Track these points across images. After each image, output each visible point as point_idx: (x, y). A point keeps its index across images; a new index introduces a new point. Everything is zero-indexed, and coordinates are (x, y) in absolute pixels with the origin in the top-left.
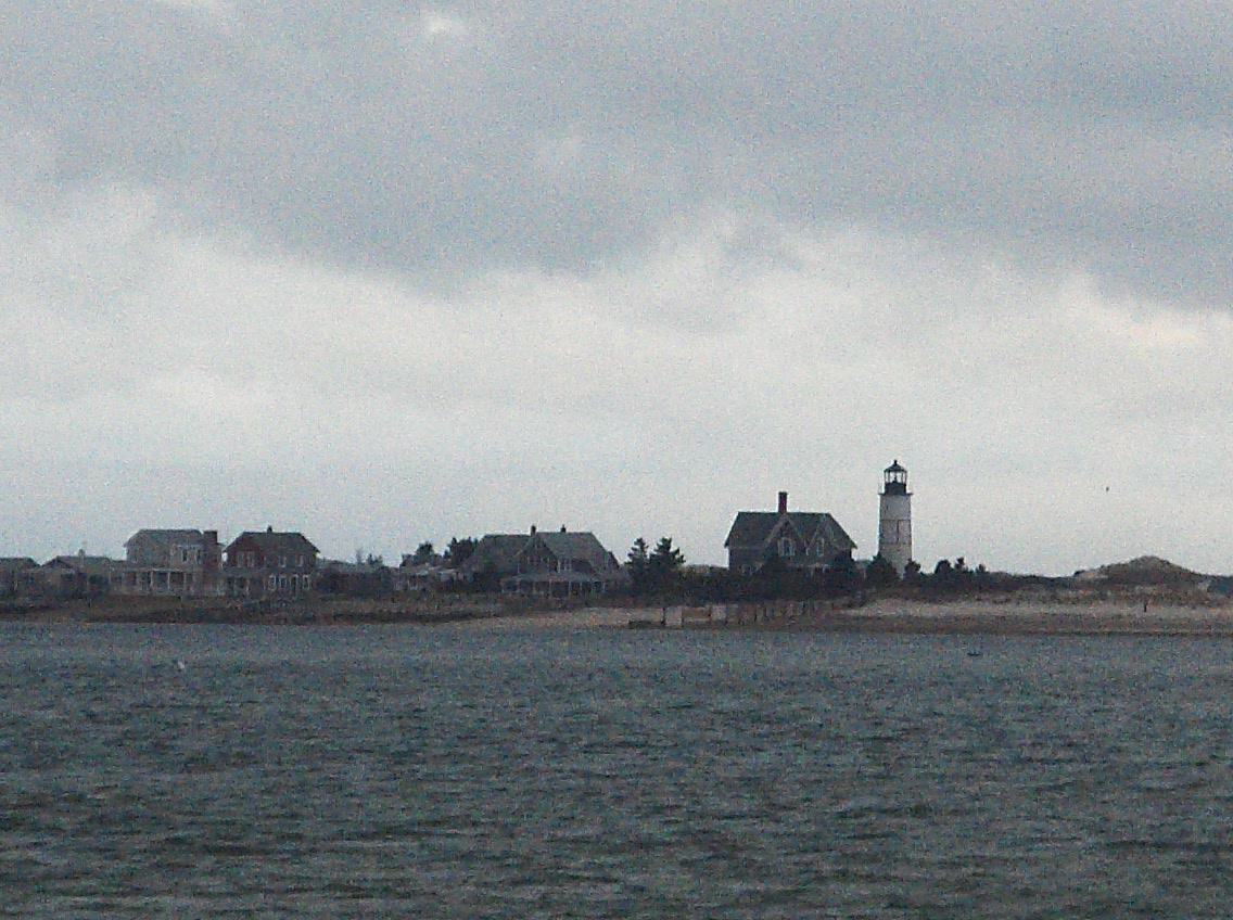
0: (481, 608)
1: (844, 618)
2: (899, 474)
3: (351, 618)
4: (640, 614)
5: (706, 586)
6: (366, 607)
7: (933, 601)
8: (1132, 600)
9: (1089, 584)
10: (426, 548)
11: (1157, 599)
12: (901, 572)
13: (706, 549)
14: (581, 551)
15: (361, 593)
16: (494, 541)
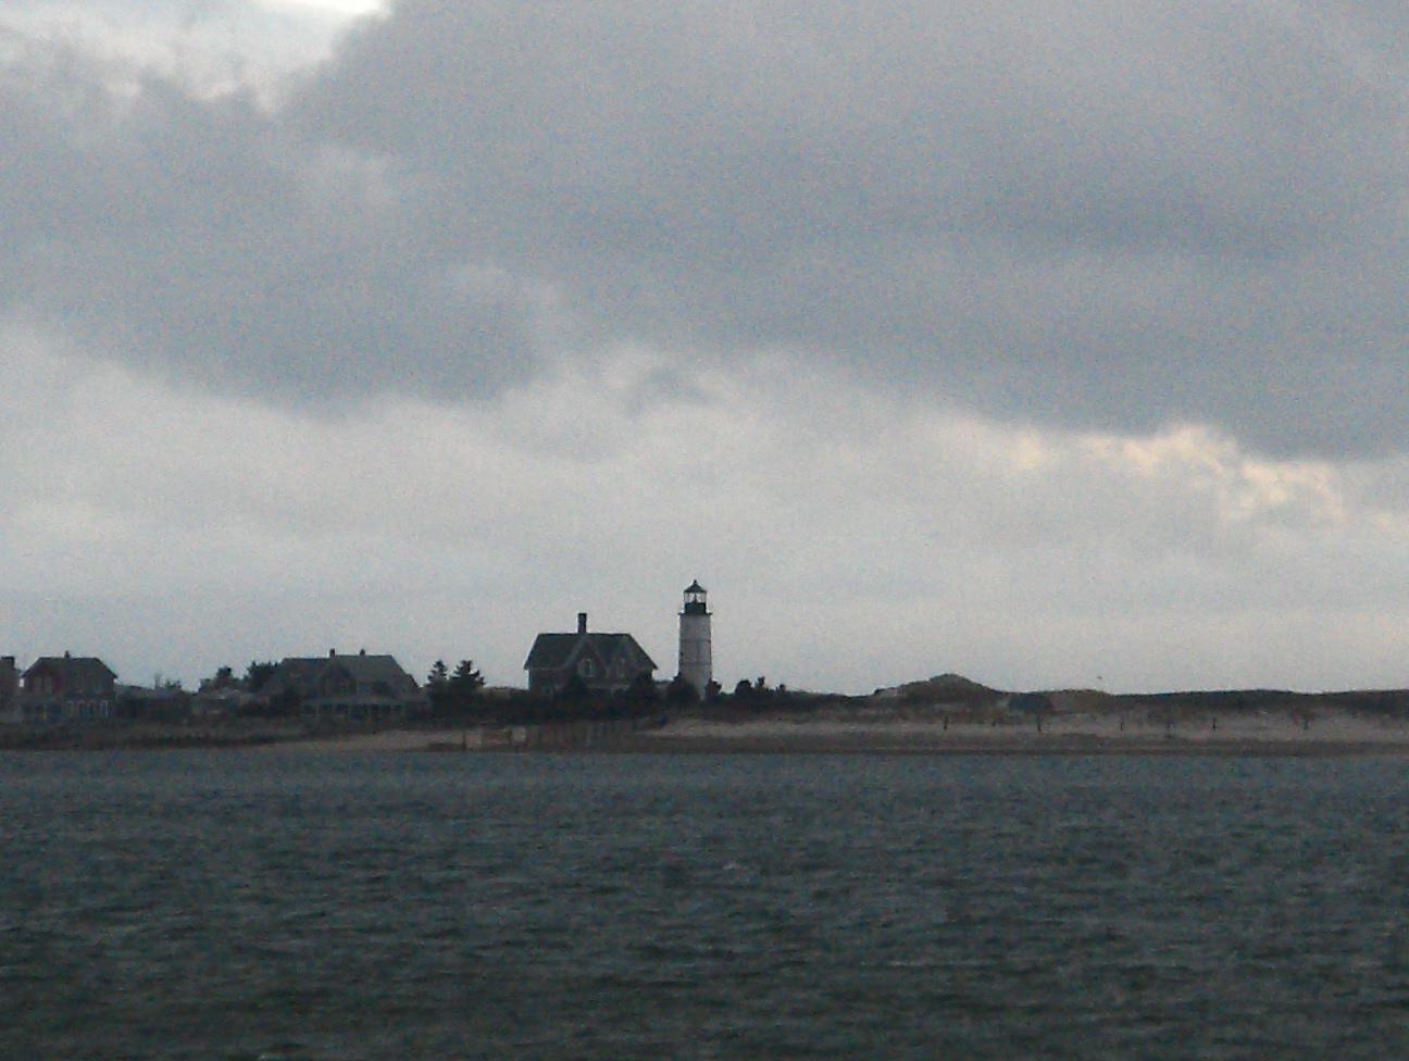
0: (282, 731)
2: (698, 595)
3: (149, 743)
5: (507, 706)
8: (930, 719)
10: (225, 673)
11: (958, 717)
13: (506, 670)
14: (381, 674)
15: (157, 717)
16: (292, 664)
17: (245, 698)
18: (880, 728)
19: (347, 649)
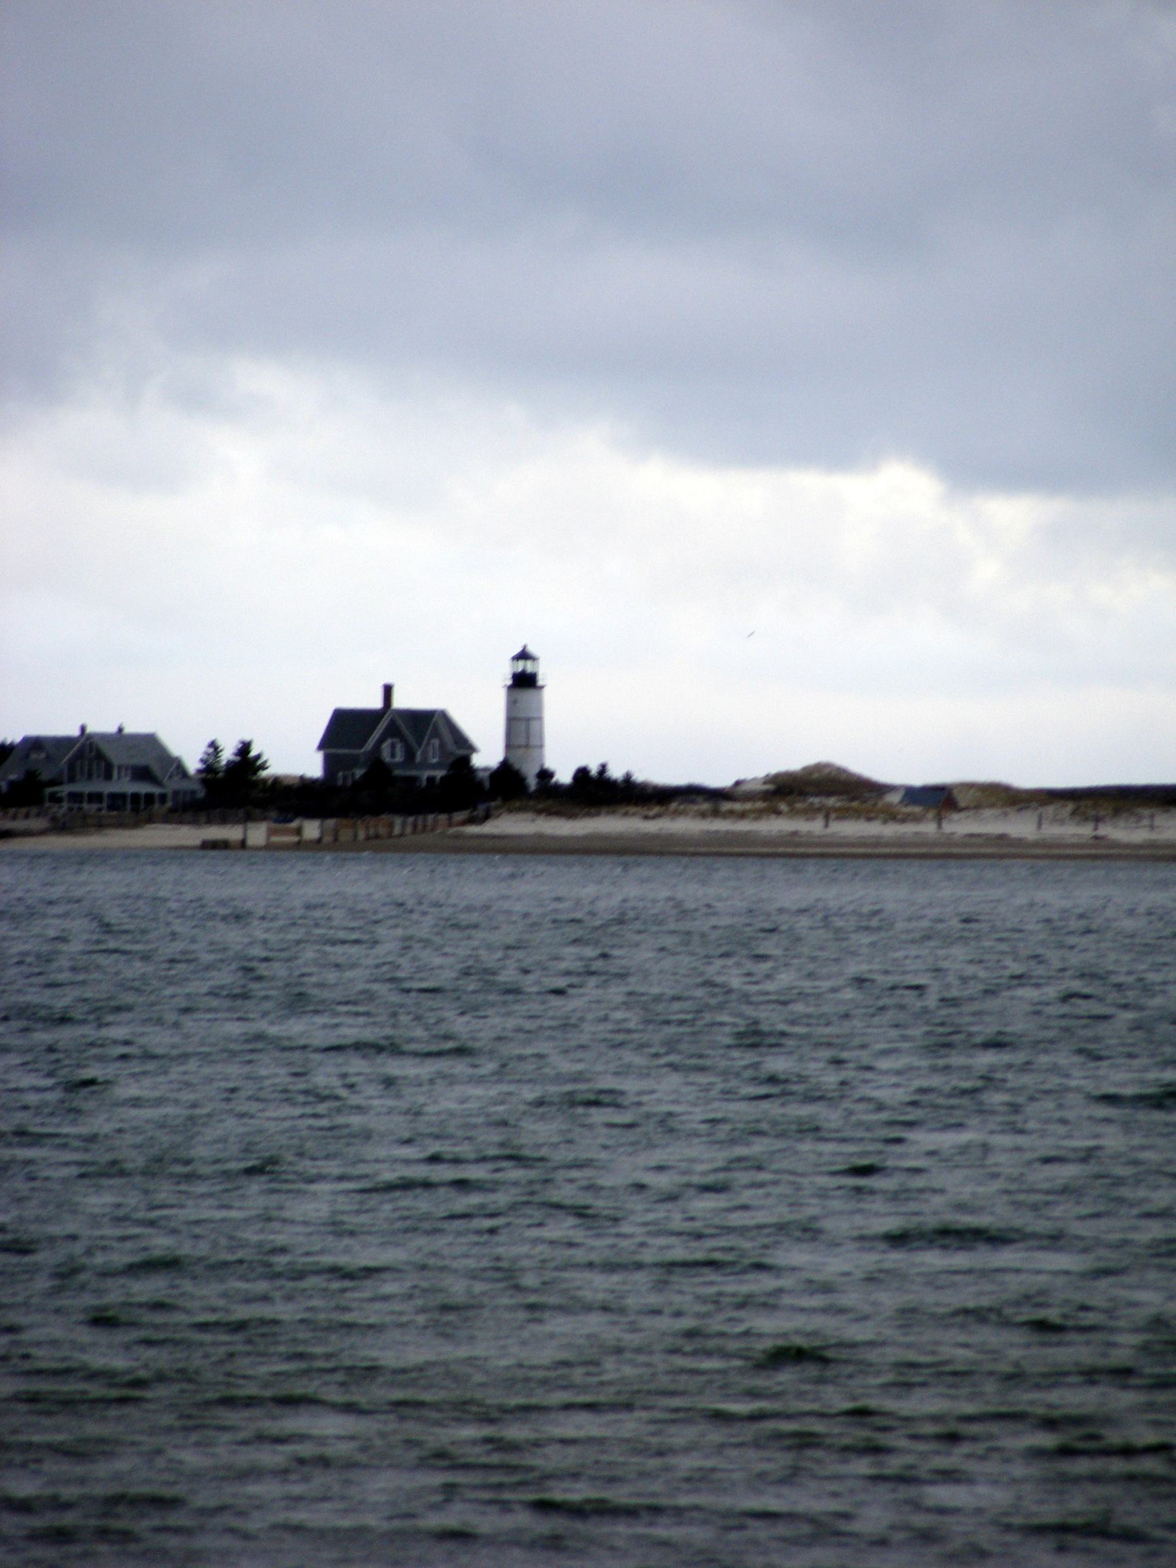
1: (457, 836)
4: (215, 832)
7: (571, 816)
8: (810, 813)
9: (750, 797)
11: (843, 814)
12: (532, 783)
13: (295, 756)
14: (145, 758)
16: (34, 744)
18: (743, 826)
19: (102, 724)
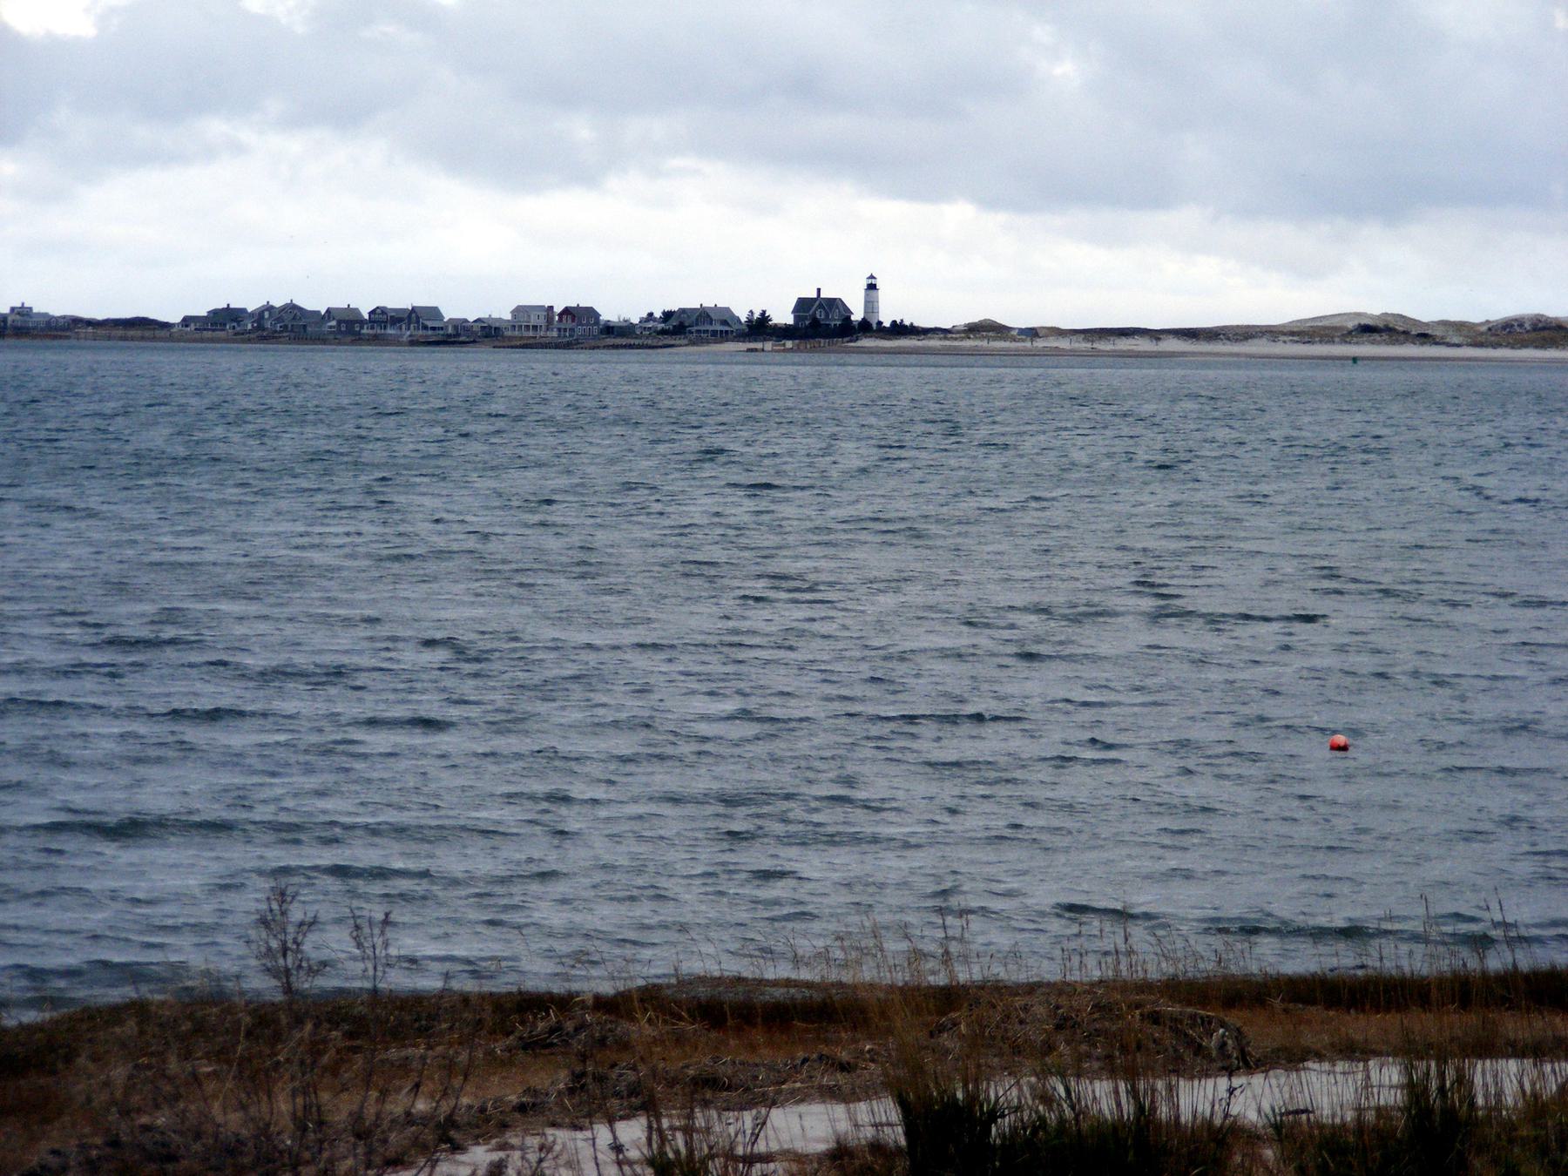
6: (624, 341)
11: (995, 339)
13: (783, 315)
14: (726, 317)
16: (683, 311)
17: (660, 326)
19: (708, 304)
